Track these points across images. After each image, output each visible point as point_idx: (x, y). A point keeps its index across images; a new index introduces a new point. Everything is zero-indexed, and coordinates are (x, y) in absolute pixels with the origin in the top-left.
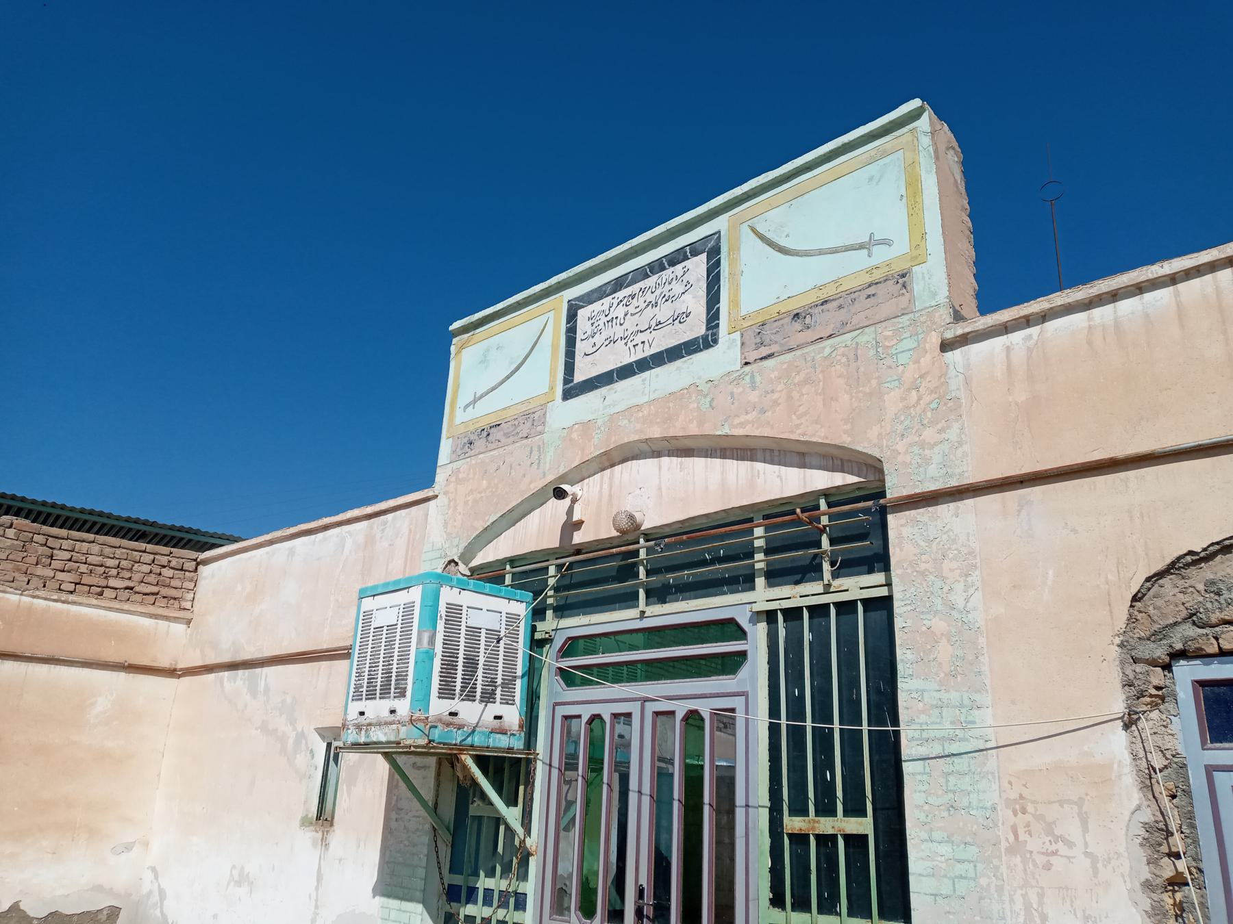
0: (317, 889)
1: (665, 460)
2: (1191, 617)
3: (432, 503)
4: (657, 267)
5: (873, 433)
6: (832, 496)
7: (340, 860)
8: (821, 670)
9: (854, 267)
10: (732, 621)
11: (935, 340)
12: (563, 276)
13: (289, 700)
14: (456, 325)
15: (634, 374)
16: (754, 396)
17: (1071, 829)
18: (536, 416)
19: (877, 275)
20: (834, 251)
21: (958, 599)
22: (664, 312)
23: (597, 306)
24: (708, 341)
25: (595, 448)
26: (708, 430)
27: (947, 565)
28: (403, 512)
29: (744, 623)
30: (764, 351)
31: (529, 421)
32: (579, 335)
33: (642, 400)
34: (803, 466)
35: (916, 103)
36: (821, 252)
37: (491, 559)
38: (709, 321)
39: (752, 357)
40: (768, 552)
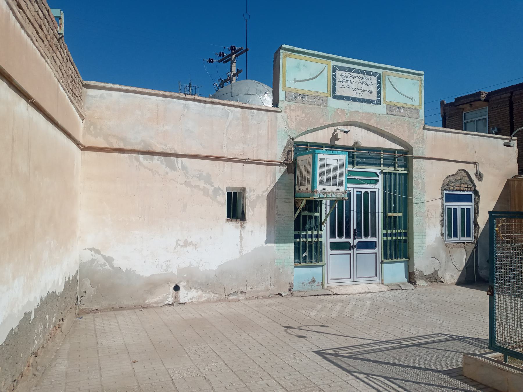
0: (241, 242)
1: (363, 130)
2: (448, 185)
3: (278, 114)
4: (362, 72)
5: (412, 141)
6: (400, 151)
7: (252, 232)
8: (397, 187)
9: (409, 102)
10: (376, 173)
11: (422, 127)
12: (334, 56)
13: (204, 174)
14: (284, 46)
15: (356, 101)
16: (389, 123)
17: (434, 214)
18: (324, 99)
19: (414, 107)
22: (365, 88)
23: (344, 73)
24: (378, 102)
25: (345, 119)
26: (379, 127)
27: (422, 170)
28: (263, 112)
29: (378, 173)
31: (320, 101)
34: (395, 143)
35: (423, 73)
36: (403, 95)
37: (304, 140)
38: (378, 97)
39: (389, 113)
40: (384, 159)
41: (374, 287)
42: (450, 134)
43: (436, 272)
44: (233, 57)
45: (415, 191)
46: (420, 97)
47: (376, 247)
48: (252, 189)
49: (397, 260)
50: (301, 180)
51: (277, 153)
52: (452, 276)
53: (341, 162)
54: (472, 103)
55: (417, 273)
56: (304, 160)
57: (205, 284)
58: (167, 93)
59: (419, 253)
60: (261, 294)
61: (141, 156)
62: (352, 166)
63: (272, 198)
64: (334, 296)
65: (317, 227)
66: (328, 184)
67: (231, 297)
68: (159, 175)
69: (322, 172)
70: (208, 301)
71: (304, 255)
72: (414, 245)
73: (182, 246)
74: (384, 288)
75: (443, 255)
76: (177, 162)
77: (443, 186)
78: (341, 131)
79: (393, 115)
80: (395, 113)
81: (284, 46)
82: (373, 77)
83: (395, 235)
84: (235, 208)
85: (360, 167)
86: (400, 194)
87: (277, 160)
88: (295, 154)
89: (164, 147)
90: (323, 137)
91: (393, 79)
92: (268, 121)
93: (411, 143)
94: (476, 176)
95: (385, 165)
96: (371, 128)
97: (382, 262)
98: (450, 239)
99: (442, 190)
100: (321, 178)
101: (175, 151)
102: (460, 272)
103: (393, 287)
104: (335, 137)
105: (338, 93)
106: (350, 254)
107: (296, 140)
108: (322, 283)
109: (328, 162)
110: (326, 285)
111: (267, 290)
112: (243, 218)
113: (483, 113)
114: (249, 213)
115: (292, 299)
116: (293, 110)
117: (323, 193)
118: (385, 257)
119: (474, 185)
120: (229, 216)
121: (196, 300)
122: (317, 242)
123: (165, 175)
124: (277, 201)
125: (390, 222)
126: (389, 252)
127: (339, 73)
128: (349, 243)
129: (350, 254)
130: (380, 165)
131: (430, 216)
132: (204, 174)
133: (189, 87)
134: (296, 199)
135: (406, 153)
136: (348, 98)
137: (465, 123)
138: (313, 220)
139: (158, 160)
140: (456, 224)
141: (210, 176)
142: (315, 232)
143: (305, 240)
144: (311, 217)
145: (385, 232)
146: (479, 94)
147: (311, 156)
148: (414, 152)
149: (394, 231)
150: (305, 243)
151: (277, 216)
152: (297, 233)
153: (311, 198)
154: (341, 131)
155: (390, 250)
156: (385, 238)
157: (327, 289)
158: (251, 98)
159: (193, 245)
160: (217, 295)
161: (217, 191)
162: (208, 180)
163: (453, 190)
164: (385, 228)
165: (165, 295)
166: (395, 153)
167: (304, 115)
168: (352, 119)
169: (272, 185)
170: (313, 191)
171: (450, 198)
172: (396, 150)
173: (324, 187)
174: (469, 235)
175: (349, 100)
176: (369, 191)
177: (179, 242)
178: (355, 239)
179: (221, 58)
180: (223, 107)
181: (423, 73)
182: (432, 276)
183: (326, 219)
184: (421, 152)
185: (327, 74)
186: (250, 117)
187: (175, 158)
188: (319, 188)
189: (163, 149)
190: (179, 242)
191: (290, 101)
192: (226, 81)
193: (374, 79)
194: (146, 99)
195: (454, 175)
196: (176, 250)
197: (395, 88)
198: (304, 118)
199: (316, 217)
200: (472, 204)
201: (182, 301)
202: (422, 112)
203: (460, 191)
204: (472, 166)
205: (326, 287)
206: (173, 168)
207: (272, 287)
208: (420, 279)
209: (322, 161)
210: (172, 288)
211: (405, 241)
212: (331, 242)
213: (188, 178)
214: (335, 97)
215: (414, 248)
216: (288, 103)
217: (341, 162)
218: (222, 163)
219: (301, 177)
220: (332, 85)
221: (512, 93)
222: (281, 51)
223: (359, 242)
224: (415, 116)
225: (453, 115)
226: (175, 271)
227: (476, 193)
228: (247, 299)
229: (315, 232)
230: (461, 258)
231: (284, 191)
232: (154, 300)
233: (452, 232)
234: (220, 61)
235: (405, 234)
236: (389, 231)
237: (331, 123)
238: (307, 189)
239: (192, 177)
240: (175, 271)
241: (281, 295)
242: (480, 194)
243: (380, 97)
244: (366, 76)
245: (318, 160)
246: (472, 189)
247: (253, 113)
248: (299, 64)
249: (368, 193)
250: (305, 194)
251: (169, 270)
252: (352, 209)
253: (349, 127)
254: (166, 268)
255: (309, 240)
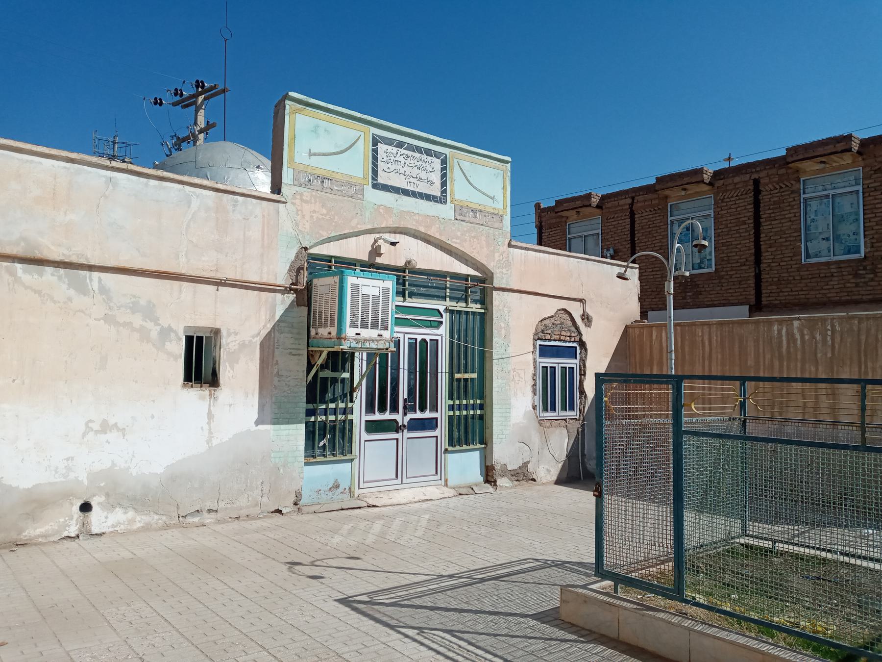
0: (209, 423)
2: (543, 331)
3: (281, 206)
4: (419, 150)
6: (474, 278)
7: (230, 405)
8: (470, 333)
10: (438, 310)
12: (374, 120)
13: (143, 302)
14: (292, 94)
16: (459, 234)
17: (522, 375)
18: (357, 188)
19: (495, 212)
20: (484, 194)
21: (507, 318)
23: (390, 148)
25: (391, 223)
26: (443, 238)
28: (254, 201)
30: (462, 218)
32: (380, 159)
33: (416, 212)
35: (509, 159)
36: (480, 191)
37: (325, 253)
38: (442, 192)
40: (451, 289)
41: (434, 491)
42: (547, 255)
43: (525, 465)
44: (201, 99)
45: (495, 340)
46: (504, 196)
47: (437, 426)
48: (232, 331)
49: (468, 448)
50: (320, 318)
51: (279, 271)
52: (549, 471)
53: (386, 291)
54: (579, 210)
55: (497, 467)
56: (324, 284)
57: (140, 499)
58: (74, 155)
59: (500, 436)
60: (244, 512)
61: (18, 266)
62: (402, 299)
63: (268, 346)
64: (370, 510)
65: (345, 395)
66: (364, 326)
67: (190, 520)
68: (55, 302)
69: (354, 306)
70: (147, 528)
71: (322, 444)
72: (494, 423)
73: (97, 432)
74: (449, 492)
75: (536, 439)
76: (91, 280)
77: (536, 334)
78: (386, 241)
79: (464, 221)
80: (467, 219)
81: (292, 94)
82: (434, 159)
83: (466, 407)
84: (200, 363)
85: (415, 300)
86: (473, 343)
87: (278, 283)
88: (310, 274)
89: (66, 252)
90: (356, 249)
91: (466, 165)
92: (264, 216)
93: (491, 266)
94: (583, 319)
95: (452, 298)
96: (432, 240)
97: (446, 450)
98: (546, 414)
99: (535, 340)
100: (353, 315)
101: (87, 259)
102: (560, 465)
103: (463, 491)
104: (376, 251)
105: (380, 180)
106: (397, 440)
107: (311, 251)
108: (350, 489)
109: (365, 291)
110: (357, 492)
111: (256, 505)
112: (214, 381)
113: (593, 225)
114: (224, 374)
115: (300, 517)
116: (306, 202)
117: (355, 340)
118: (451, 442)
119: (580, 334)
120: (188, 378)
121: (122, 527)
122: (344, 421)
123: (65, 303)
124: (277, 352)
125: (459, 387)
126: (456, 434)
127: (382, 147)
128: (395, 421)
129: (397, 440)
130: (444, 298)
131: (517, 379)
132: (143, 302)
133: (114, 143)
134: (310, 349)
135: (483, 281)
136: (396, 190)
137: (570, 239)
138: (339, 386)
139: (52, 275)
140: (555, 391)
141: (154, 306)
142: (342, 405)
143: (324, 418)
144: (335, 380)
145: (451, 402)
146: (589, 196)
147: (337, 279)
148: (495, 281)
149: (464, 402)
150: (324, 423)
151: (276, 379)
152: (311, 406)
153: (336, 349)
154: (386, 241)
155: (459, 432)
156: (451, 413)
157: (358, 498)
158: (232, 174)
159: (118, 429)
160: (164, 518)
161: (166, 333)
162: (150, 312)
163: (549, 340)
164: (451, 397)
165: (62, 520)
166: (467, 280)
167: (324, 211)
168: (403, 224)
169: (270, 326)
170: (340, 338)
171: (545, 351)
172: (468, 275)
173: (358, 330)
174: (572, 408)
175: (398, 193)
176: (428, 338)
177: (90, 425)
178: (405, 414)
179: (178, 98)
180: (180, 186)
181: (509, 159)
182: (519, 471)
183: (360, 384)
184: (504, 281)
185: (363, 148)
186: (230, 208)
187: (87, 273)
188: (350, 332)
189: (63, 255)
190: (90, 425)
191: (301, 185)
192: (186, 139)
193: (437, 163)
194: (32, 162)
195: (552, 317)
196: (85, 439)
197: (468, 181)
198: (326, 215)
199: (343, 380)
200: (577, 361)
201: (95, 530)
202: (507, 219)
203: (559, 342)
204: (578, 304)
205: (356, 495)
206: (83, 290)
207: (265, 499)
208: (502, 476)
209: (356, 288)
210: (76, 508)
211: (481, 417)
212: (366, 421)
213: (111, 308)
214: (376, 186)
215: (494, 428)
216: (298, 189)
217: (386, 291)
218: (176, 284)
219: (320, 312)
220: (371, 165)
221: (633, 198)
222: (287, 102)
223: (411, 419)
224: (497, 225)
225: (552, 227)
226: (83, 477)
227: (582, 344)
228: (219, 522)
229: (342, 405)
230: (560, 443)
231: (290, 335)
232: (39, 531)
233: (548, 404)
234: (175, 104)
235: (481, 407)
236: (457, 402)
237: (369, 227)
238: (330, 333)
239: (119, 308)
240: (83, 477)
241: (280, 512)
242: (588, 346)
243: (445, 191)
244: (424, 156)
245: (349, 286)
246: (577, 339)
247: (237, 201)
248: (317, 127)
249: (427, 343)
250: (326, 342)
251: (72, 476)
252: (401, 366)
253: (398, 235)
254: (64, 471)
255: (332, 418)
